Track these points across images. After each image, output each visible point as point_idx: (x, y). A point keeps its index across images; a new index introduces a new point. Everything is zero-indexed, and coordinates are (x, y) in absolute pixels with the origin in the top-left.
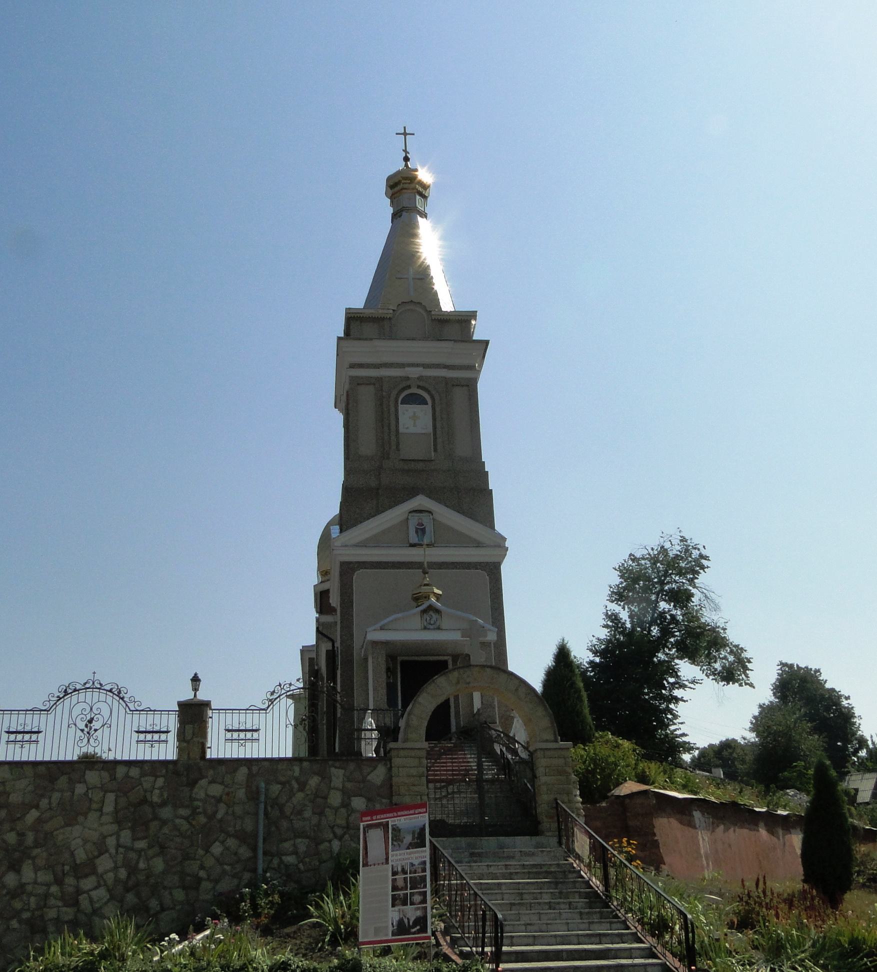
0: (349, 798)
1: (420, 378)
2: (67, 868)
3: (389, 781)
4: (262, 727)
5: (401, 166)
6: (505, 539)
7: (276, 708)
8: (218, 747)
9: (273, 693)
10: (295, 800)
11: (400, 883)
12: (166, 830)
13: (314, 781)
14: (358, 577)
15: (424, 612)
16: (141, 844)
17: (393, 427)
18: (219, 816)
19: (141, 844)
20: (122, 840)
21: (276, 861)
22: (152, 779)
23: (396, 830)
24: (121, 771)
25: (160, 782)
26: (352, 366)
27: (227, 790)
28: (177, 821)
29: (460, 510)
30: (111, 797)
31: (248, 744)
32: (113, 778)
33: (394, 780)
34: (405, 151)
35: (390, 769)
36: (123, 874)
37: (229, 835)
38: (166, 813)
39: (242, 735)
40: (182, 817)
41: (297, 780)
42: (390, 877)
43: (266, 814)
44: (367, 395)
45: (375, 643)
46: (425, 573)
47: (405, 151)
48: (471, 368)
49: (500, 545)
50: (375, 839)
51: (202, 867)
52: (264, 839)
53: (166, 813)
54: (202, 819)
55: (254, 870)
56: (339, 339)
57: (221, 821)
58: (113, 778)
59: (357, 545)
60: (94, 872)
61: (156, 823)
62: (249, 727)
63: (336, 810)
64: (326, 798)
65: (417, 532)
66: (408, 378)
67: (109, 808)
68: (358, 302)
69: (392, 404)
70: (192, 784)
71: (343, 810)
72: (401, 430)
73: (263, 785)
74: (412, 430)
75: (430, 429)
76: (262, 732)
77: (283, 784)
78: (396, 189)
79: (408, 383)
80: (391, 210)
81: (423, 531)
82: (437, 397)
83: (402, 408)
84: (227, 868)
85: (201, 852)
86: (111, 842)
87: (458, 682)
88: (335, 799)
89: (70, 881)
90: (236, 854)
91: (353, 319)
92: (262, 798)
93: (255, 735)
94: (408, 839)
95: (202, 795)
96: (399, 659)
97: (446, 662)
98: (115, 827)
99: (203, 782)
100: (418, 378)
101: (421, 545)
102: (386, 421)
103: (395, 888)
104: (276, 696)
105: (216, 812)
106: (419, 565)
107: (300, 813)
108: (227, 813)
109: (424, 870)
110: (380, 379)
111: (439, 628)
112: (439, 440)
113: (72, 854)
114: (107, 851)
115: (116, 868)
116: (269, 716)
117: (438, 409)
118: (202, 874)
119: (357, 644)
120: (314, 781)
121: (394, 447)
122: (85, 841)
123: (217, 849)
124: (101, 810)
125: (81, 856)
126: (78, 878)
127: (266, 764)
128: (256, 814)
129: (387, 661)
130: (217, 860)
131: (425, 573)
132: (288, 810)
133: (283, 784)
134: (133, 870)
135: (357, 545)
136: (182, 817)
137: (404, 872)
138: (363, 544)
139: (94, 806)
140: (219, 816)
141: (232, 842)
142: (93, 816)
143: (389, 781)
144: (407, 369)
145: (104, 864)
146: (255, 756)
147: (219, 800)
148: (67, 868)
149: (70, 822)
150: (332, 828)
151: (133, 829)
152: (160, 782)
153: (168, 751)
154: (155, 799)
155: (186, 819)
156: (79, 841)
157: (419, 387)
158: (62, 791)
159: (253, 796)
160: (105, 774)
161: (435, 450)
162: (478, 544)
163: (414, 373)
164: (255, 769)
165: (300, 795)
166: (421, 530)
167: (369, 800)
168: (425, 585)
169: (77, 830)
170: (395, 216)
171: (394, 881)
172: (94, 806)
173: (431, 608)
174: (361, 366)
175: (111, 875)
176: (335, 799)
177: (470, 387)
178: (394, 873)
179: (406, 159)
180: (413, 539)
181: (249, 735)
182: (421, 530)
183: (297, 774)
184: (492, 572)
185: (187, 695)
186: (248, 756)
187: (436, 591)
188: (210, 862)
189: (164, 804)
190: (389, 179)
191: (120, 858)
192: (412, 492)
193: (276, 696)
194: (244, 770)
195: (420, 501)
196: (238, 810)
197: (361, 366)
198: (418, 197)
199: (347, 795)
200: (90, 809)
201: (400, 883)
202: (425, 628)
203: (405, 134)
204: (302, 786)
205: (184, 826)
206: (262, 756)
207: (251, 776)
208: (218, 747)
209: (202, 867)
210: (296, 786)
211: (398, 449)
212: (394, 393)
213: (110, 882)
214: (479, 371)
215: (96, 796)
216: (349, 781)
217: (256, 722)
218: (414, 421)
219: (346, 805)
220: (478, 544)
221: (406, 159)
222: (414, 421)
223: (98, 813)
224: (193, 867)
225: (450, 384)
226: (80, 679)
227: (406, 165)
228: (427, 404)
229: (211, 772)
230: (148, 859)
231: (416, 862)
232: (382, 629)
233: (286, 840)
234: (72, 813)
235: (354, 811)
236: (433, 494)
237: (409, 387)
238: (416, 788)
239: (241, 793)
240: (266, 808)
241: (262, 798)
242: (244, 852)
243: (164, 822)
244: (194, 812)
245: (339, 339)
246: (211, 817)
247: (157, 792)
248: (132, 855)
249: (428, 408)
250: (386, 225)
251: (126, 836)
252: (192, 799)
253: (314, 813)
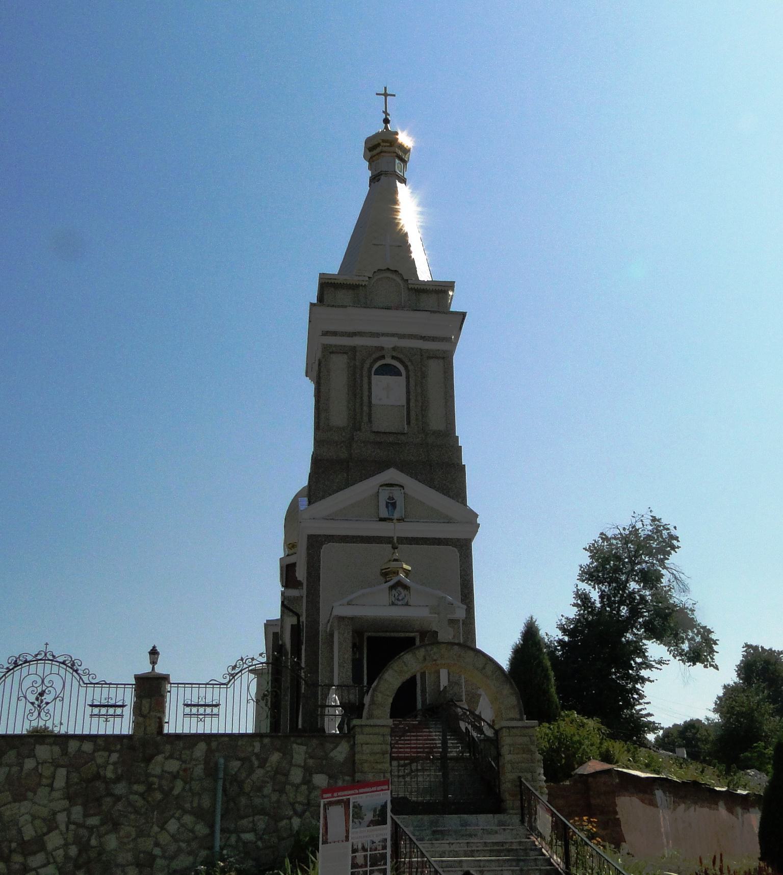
0: (311, 775)
2: (14, 845)
3: (351, 759)
4: (222, 702)
5: (380, 128)
6: (477, 516)
7: (238, 682)
8: (177, 721)
9: (234, 668)
10: (254, 777)
11: (360, 861)
12: (120, 806)
13: (275, 757)
14: (327, 552)
15: (392, 588)
16: (94, 821)
17: (365, 398)
18: (176, 792)
19: (94, 821)
20: (74, 817)
21: (233, 839)
22: (106, 754)
23: (358, 807)
24: (73, 746)
25: (114, 757)
26: (326, 333)
27: (184, 766)
28: (131, 797)
29: (430, 484)
30: (62, 772)
31: (208, 720)
32: (65, 752)
33: (357, 757)
34: (385, 112)
35: (353, 747)
36: (73, 851)
37: (185, 812)
38: (120, 789)
39: (201, 710)
40: (136, 793)
41: (257, 756)
42: (350, 855)
43: (224, 790)
44: (339, 363)
45: (341, 619)
46: (395, 548)
47: (385, 112)
48: (447, 339)
49: (471, 522)
50: (336, 815)
51: (157, 844)
52: (222, 816)
53: (120, 789)
54: (158, 796)
55: (211, 848)
56: (312, 305)
57: (178, 796)
58: (65, 752)
59: (325, 519)
60: (42, 847)
61: (108, 799)
62: (209, 701)
63: (297, 787)
64: (286, 775)
65: (387, 507)
66: (382, 348)
67: (60, 783)
68: (333, 267)
69: (365, 373)
70: (148, 760)
71: (304, 787)
72: (373, 402)
73: (222, 761)
75: (404, 403)
76: (222, 707)
77: (243, 760)
78: (375, 152)
80: (369, 174)
81: (394, 505)
82: (411, 368)
83: (375, 378)
84: (183, 845)
85: (156, 829)
86: (62, 818)
87: (425, 659)
88: (296, 776)
89: (17, 858)
90: (192, 831)
91: (327, 285)
92: (221, 775)
93: (215, 710)
94: (369, 816)
95: (158, 771)
96: (366, 635)
97: (413, 639)
98: (66, 803)
99: (160, 758)
101: (392, 520)
102: (358, 392)
103: (354, 865)
104: (237, 670)
105: (172, 789)
106: (388, 540)
107: (260, 789)
108: (184, 789)
109: (384, 848)
110: (354, 349)
111: (407, 604)
112: (413, 414)
113: (20, 831)
114: (57, 827)
115: (66, 845)
116: (230, 690)
117: (412, 382)
118: (157, 851)
119: (323, 619)
120: (275, 757)
121: (365, 419)
122: (34, 817)
123: (172, 826)
124: (51, 786)
125: (29, 833)
126: (25, 855)
127: (227, 739)
128: (214, 790)
129: (353, 637)
130: (173, 836)
131: (395, 548)
132: (247, 787)
133: (243, 760)
134: (84, 847)
135: (325, 519)
136: (136, 793)
137: (364, 849)
138: (330, 518)
139: (45, 781)
140: (176, 792)
141: (188, 819)
142: (43, 792)
143: (351, 759)
144: (382, 338)
145: (54, 841)
146: (214, 731)
147: (175, 776)
148: (14, 845)
149: (19, 798)
150: (292, 805)
151: (85, 805)
152: (114, 757)
153: (124, 725)
154: (110, 774)
155: (142, 795)
156: (27, 817)
157: (393, 357)
158: (10, 766)
159: (211, 771)
160: (56, 749)
161: (409, 423)
162: (449, 521)
163: (388, 343)
164: (214, 745)
165: (260, 772)
166: (392, 504)
167: (330, 777)
168: (396, 560)
169: (25, 806)
170: (374, 179)
171: (354, 858)
172: (45, 781)
173: (399, 584)
174: (335, 334)
175: (61, 852)
176: (296, 776)
177: (446, 360)
178: (354, 851)
179: (386, 121)
180: (384, 513)
181: (208, 710)
182: (392, 504)
183: (257, 749)
184: (464, 548)
185: (145, 668)
186: (208, 731)
187: (405, 566)
188: (164, 838)
189: (118, 779)
190: (368, 141)
191: (70, 836)
192: (382, 466)
193: (237, 670)
194: (202, 746)
195: (392, 475)
196: (196, 786)
197: (335, 334)
198: (397, 161)
199: (308, 772)
200: (39, 785)
201: (360, 861)
202: (393, 604)
203: (386, 95)
204: (263, 763)
205: (140, 802)
206: (222, 731)
207: (210, 751)
208: (177, 721)
209: (157, 844)
210: (256, 763)
211: (370, 421)
212: (368, 362)
213: (60, 860)
214: (455, 344)
215: (47, 771)
216: (311, 757)
217: (216, 697)
218: (388, 393)
219: (307, 781)
220: (449, 521)
221: (386, 121)
222: (388, 393)
223: (48, 789)
224: (146, 844)
226: (32, 649)
227: (386, 128)
228: (399, 374)
229: (168, 747)
230: (100, 836)
231: (377, 840)
232: (348, 604)
233: (243, 818)
234: (20, 790)
235: (315, 788)
236: (405, 467)
237: (383, 357)
238: (379, 766)
239: (199, 770)
240: (224, 784)
241: (221, 775)
242: (201, 829)
243: (118, 798)
244: (150, 788)
245: (312, 305)
246: (167, 794)
247: (111, 767)
248: (83, 832)
249: (402, 380)
250: (363, 188)
251: (77, 812)
252: (148, 775)
253: (274, 790)
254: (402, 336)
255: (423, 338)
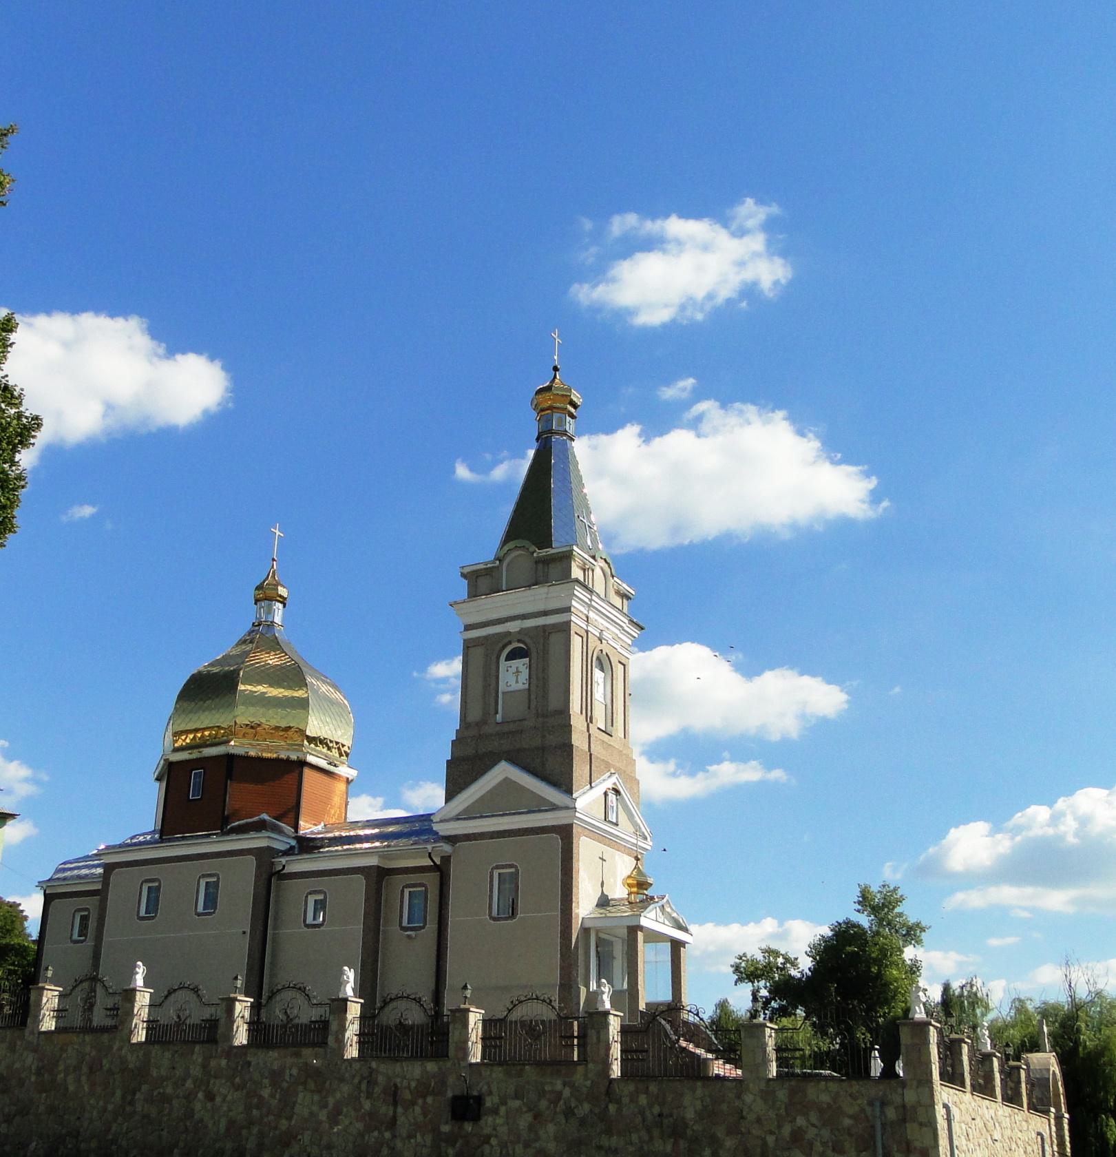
1: (522, 631)
26: (468, 628)
44: (478, 652)
66: (509, 633)
74: (515, 687)
79: (507, 640)
83: (503, 664)
100: (519, 632)
102: (491, 678)
112: (533, 697)
135: (457, 818)
157: (519, 641)
162: (554, 808)
163: (513, 627)
220: (554, 808)
222: (514, 676)
225: (546, 631)
237: (510, 643)
254: (524, 617)
255: (545, 613)
